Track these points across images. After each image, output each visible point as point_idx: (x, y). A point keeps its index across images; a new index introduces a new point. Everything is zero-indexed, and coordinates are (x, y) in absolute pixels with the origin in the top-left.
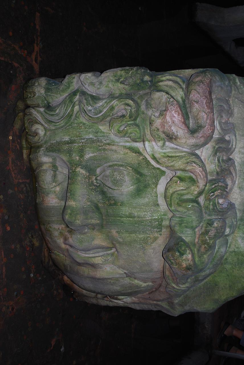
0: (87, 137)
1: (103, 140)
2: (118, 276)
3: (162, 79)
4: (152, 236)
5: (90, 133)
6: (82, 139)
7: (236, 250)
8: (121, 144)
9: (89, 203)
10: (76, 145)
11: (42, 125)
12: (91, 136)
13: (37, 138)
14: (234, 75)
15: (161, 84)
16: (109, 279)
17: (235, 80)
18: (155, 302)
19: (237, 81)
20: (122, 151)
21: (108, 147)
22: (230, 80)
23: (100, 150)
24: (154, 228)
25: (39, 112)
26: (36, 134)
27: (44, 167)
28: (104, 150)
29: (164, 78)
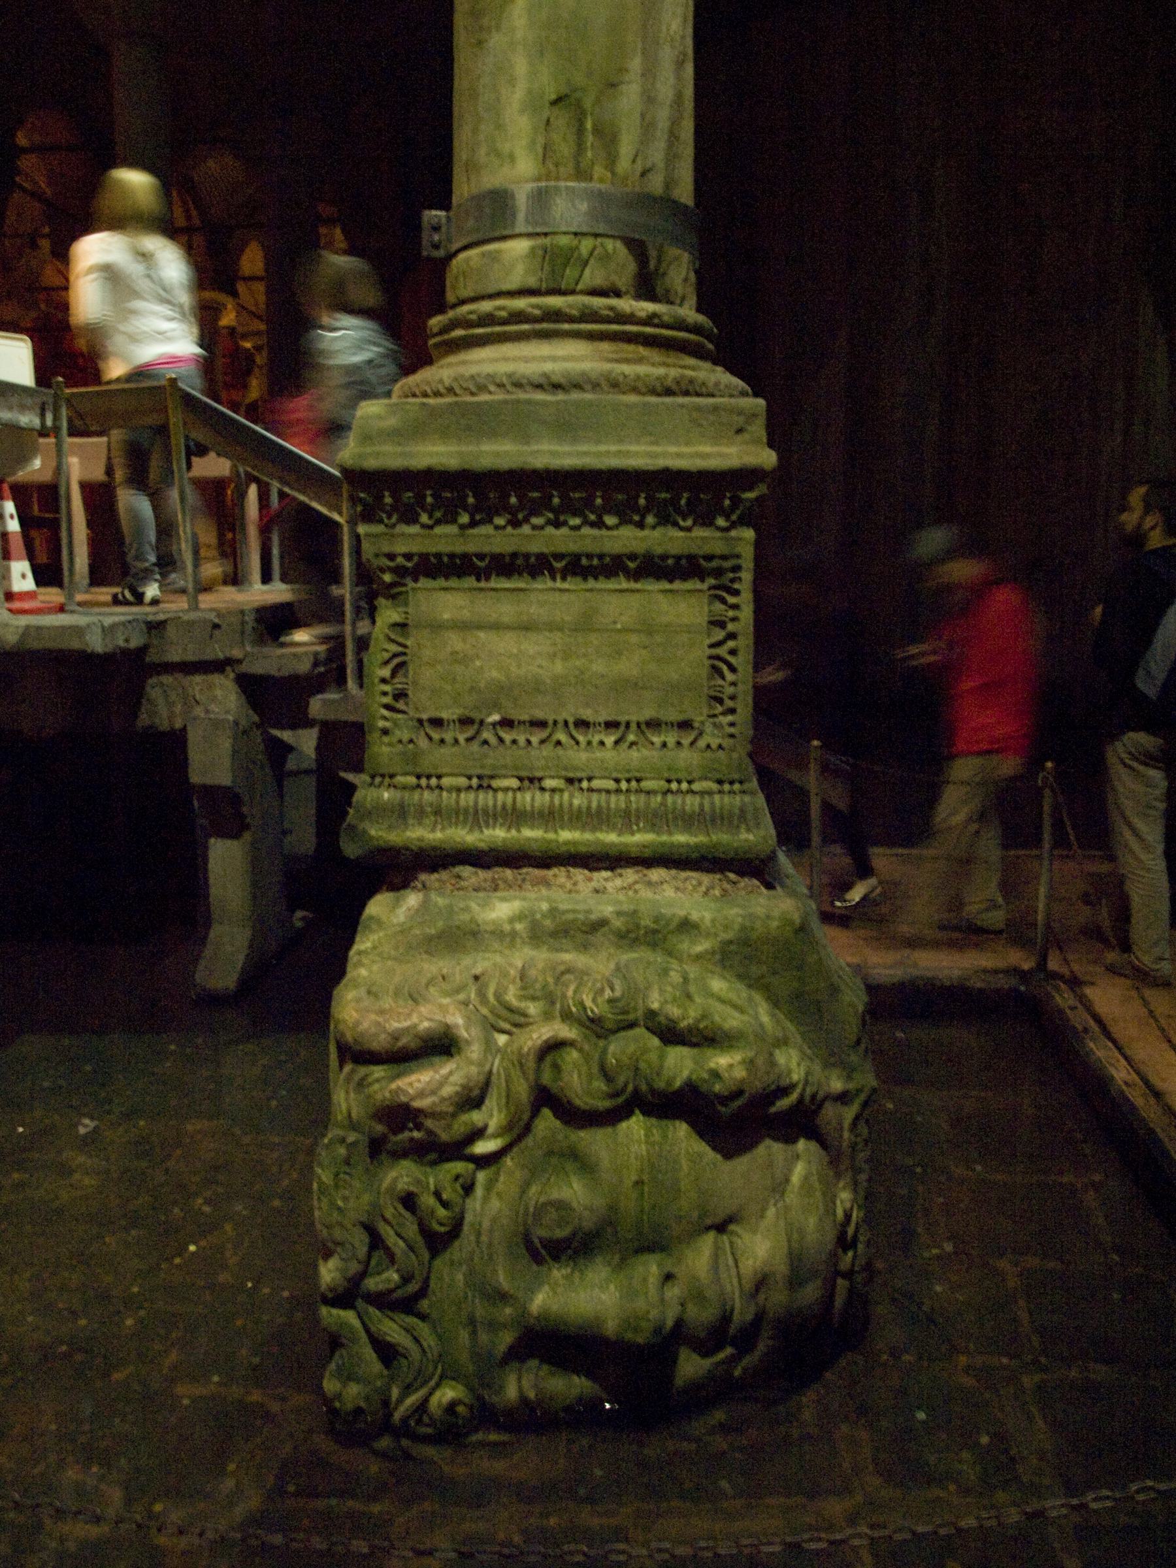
0: (461, 1284)
1: (470, 1249)
2: (782, 1223)
3: (344, 1111)
4: (683, 1145)
5: (453, 1280)
6: (466, 1298)
7: (718, 957)
8: (478, 1207)
9: (612, 1287)
10: (480, 1312)
11: (431, 1394)
12: (460, 1277)
13: (460, 1409)
14: (352, 953)
15: (354, 1115)
16: (789, 1241)
17: (359, 953)
18: (846, 1135)
19: (362, 947)
20: (495, 1204)
21: (484, 1238)
22: (360, 964)
23: (491, 1258)
24: (665, 1137)
25: (400, 1401)
26: (451, 1407)
27: (532, 1395)
28: (490, 1245)
29: (344, 1106)
